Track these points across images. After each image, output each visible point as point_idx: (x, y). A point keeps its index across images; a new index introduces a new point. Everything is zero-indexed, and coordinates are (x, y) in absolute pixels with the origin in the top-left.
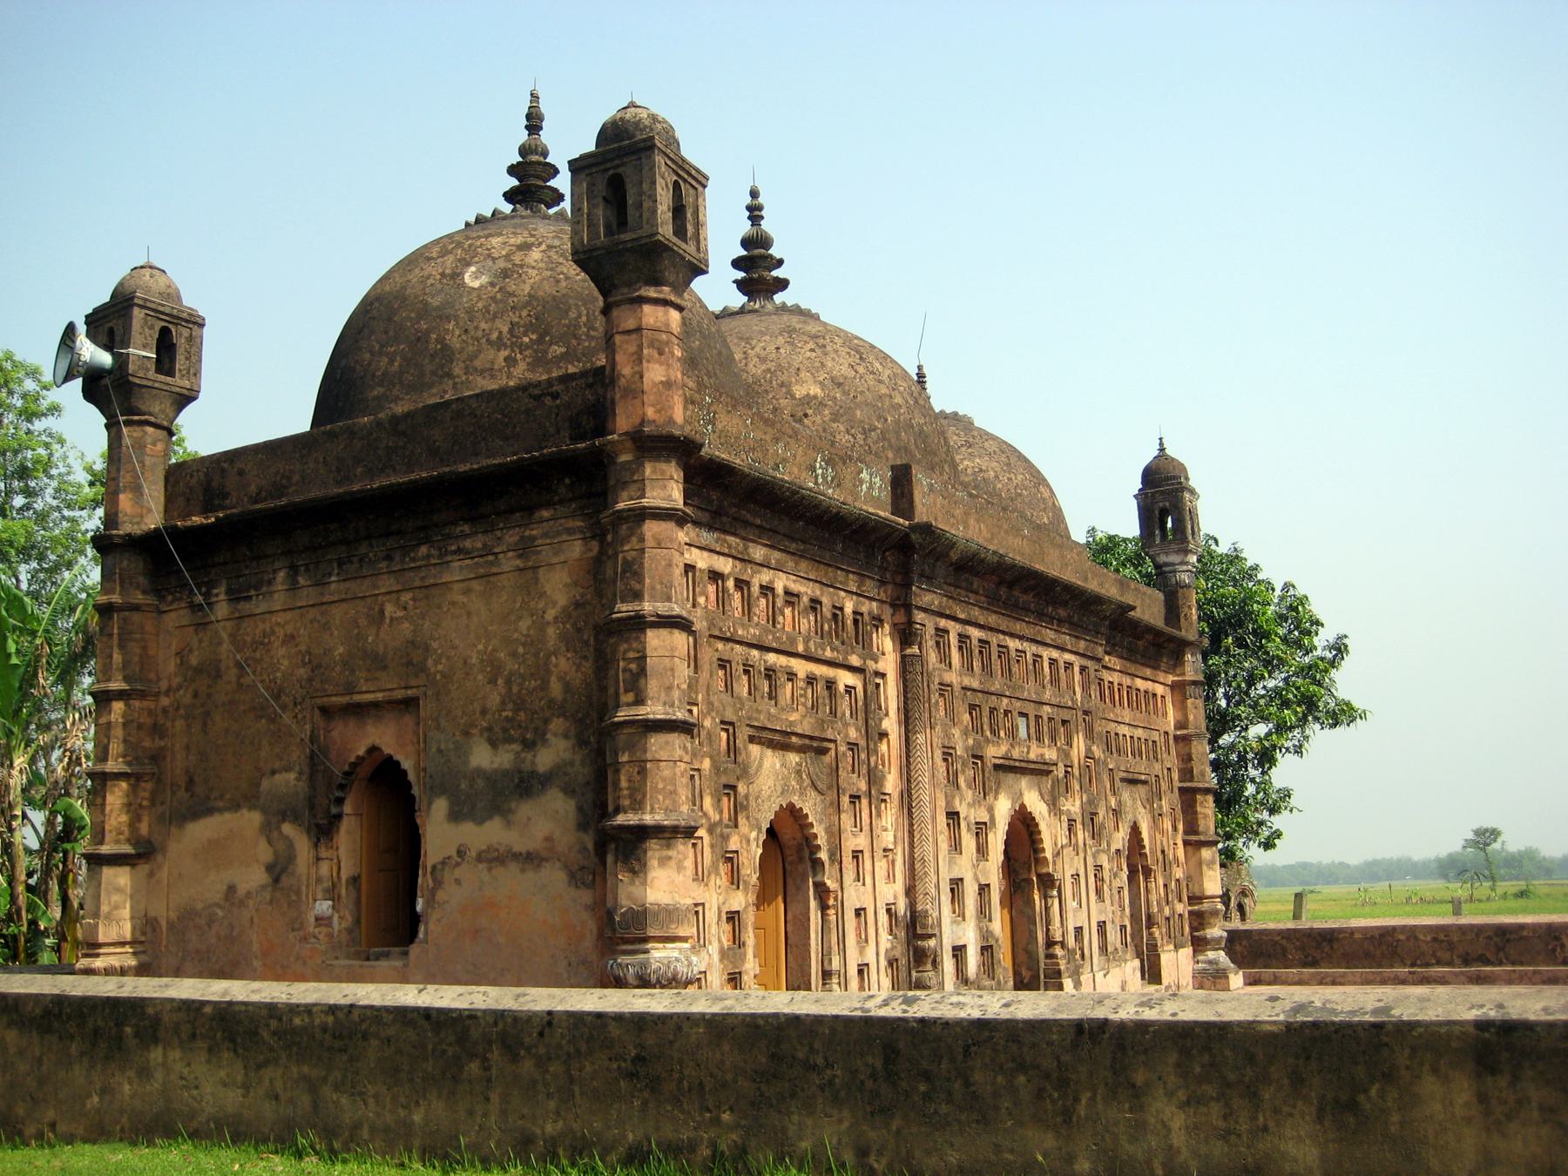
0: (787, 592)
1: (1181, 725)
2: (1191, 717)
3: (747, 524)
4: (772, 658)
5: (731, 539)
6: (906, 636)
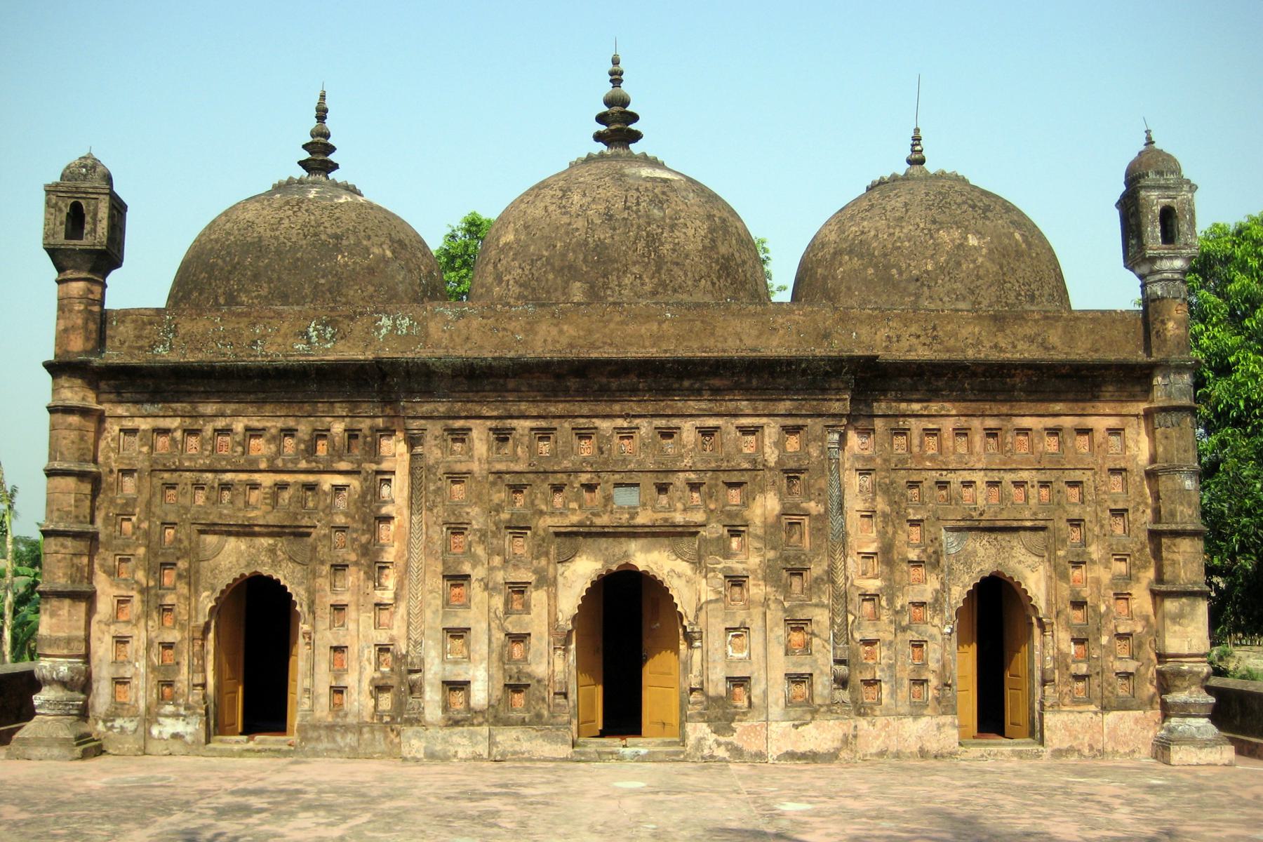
0: (247, 429)
1: (1153, 459)
2: (1160, 449)
3: (189, 393)
4: (228, 477)
5: (174, 405)
6: (413, 441)
